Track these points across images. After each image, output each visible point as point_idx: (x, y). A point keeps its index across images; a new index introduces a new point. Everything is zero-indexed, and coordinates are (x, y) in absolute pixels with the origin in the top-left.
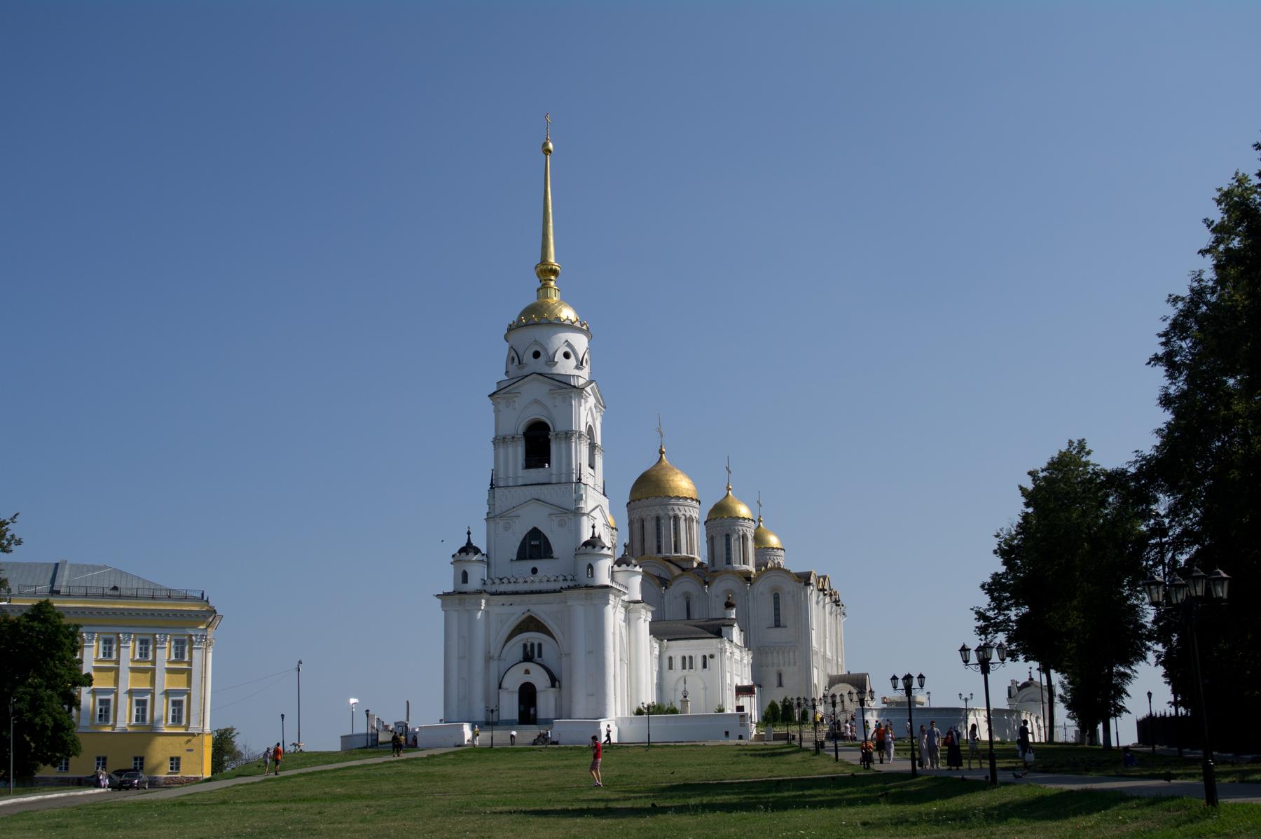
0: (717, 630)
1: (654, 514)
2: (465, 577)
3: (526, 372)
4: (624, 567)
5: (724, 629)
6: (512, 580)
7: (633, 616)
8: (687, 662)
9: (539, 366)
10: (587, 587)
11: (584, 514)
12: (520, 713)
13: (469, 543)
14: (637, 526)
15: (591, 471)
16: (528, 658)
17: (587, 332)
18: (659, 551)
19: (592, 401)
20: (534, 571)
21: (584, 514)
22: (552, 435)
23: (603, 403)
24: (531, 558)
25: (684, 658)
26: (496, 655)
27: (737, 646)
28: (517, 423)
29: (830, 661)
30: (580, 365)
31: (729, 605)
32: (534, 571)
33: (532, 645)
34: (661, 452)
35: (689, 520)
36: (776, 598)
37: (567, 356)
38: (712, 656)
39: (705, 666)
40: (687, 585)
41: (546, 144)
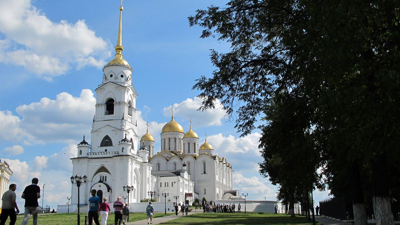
0: (178, 173)
1: (168, 137)
4: (142, 150)
5: (181, 173)
7: (144, 167)
8: (166, 185)
9: (112, 79)
10: (122, 156)
11: (124, 130)
13: (84, 140)
14: (163, 141)
15: (129, 116)
16: (100, 181)
17: (131, 69)
18: (170, 149)
19: (131, 92)
20: (106, 150)
21: (124, 130)
22: (115, 103)
23: (136, 94)
24: (105, 146)
25: (165, 183)
26: (90, 181)
27: (186, 180)
28: (104, 100)
29: (225, 186)
30: (127, 80)
31: (184, 165)
32: (106, 150)
33: (103, 177)
34: (172, 118)
35: (180, 139)
36: (204, 164)
37: (122, 76)
38: (175, 182)
39: (172, 186)
40: (176, 160)
41: (121, 7)
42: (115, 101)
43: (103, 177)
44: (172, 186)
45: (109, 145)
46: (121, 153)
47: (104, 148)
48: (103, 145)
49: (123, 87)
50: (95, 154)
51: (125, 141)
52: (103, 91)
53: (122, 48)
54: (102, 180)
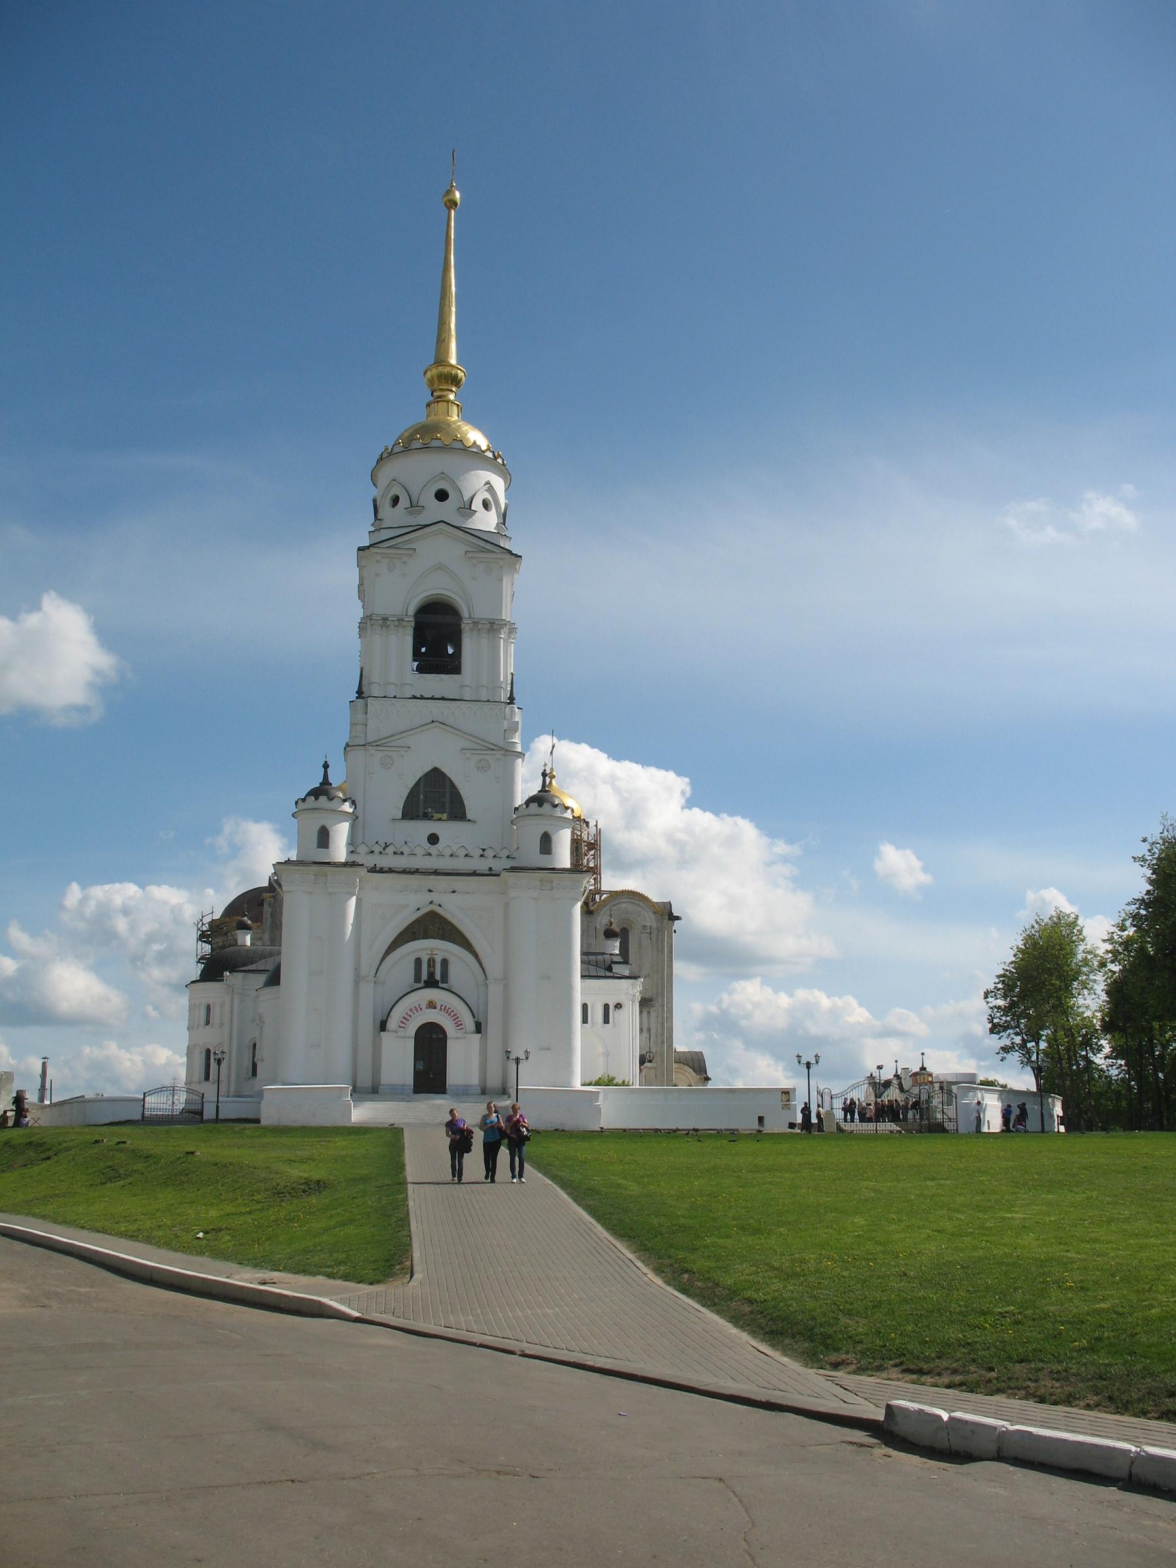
2: (324, 839)
3: (422, 519)
6: (406, 850)
9: (446, 511)
12: (417, 1074)
16: (431, 983)
20: (433, 839)
22: (466, 626)
24: (426, 817)
31: (610, 934)
32: (433, 839)
33: (431, 962)
37: (486, 505)
38: (618, 1006)
39: (606, 1020)
41: (449, 192)
42: (465, 613)
43: (431, 962)
44: (606, 1020)
45: (421, 814)
46: (534, 857)
47: (424, 828)
48: (414, 809)
49: (508, 556)
50: (390, 850)
51: (540, 805)
52: (405, 559)
53: (461, 374)
54: (438, 977)
